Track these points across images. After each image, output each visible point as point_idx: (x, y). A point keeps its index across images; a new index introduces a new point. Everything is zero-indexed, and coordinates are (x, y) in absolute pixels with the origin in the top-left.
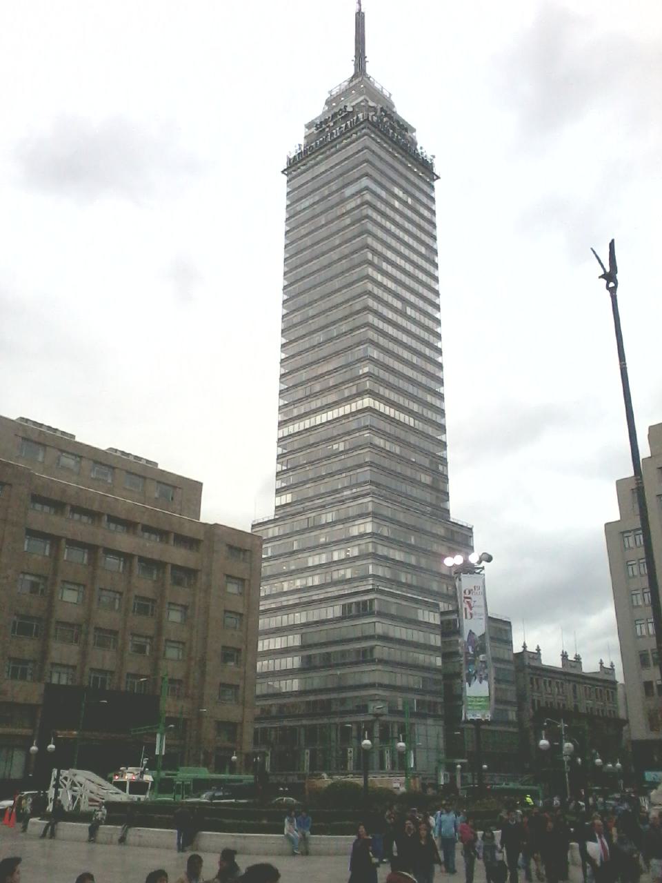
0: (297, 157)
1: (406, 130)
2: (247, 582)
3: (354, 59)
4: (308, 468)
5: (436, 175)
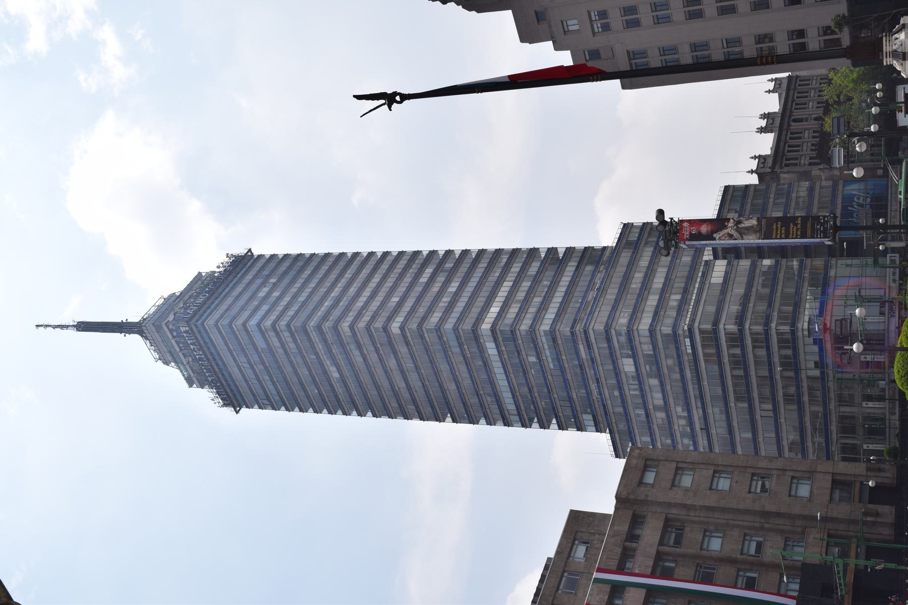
0: (222, 396)
2: (680, 465)
3: (123, 334)
4: (556, 396)
5: (247, 252)
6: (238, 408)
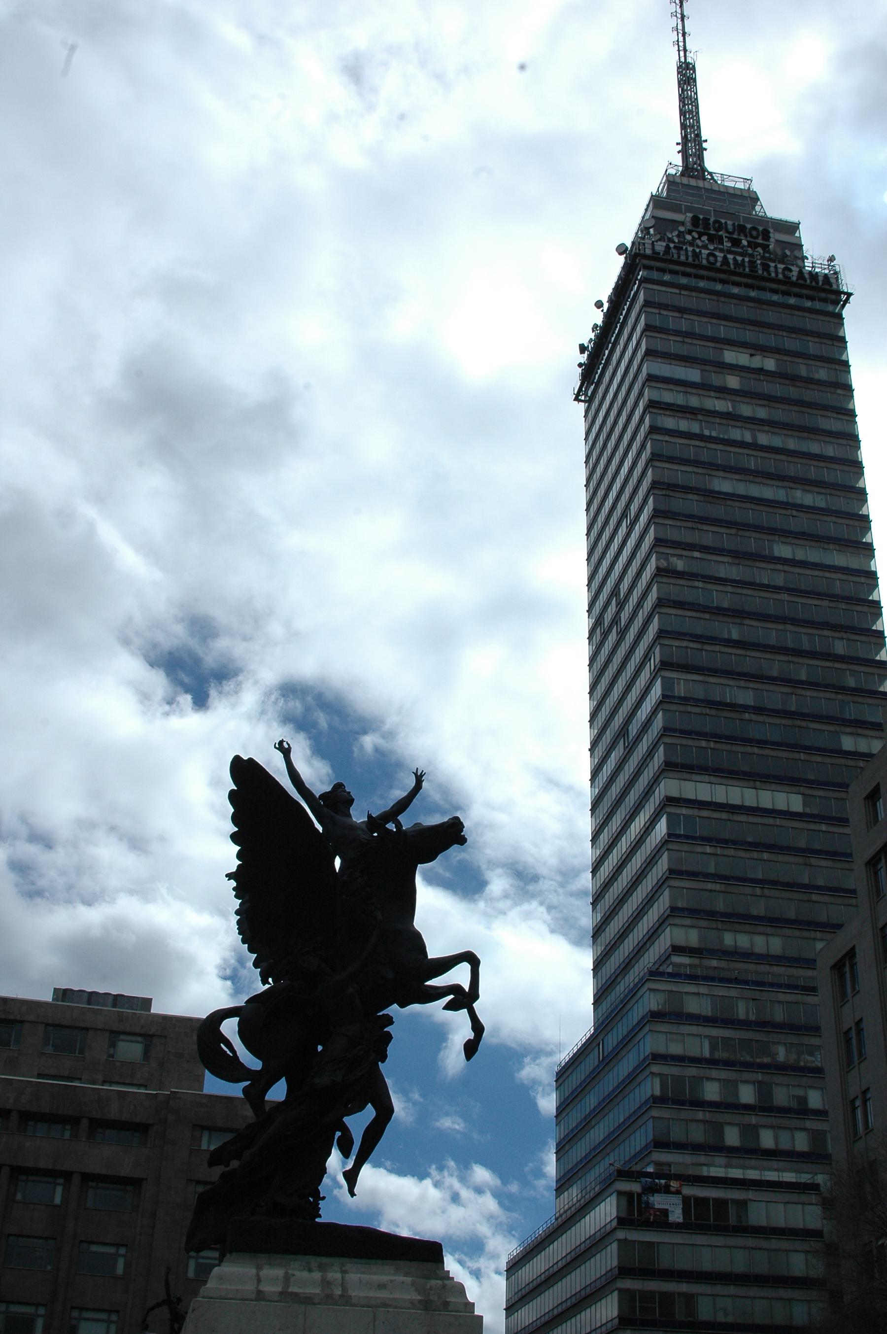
1: (766, 235)
5: (845, 293)
6: (583, 398)
